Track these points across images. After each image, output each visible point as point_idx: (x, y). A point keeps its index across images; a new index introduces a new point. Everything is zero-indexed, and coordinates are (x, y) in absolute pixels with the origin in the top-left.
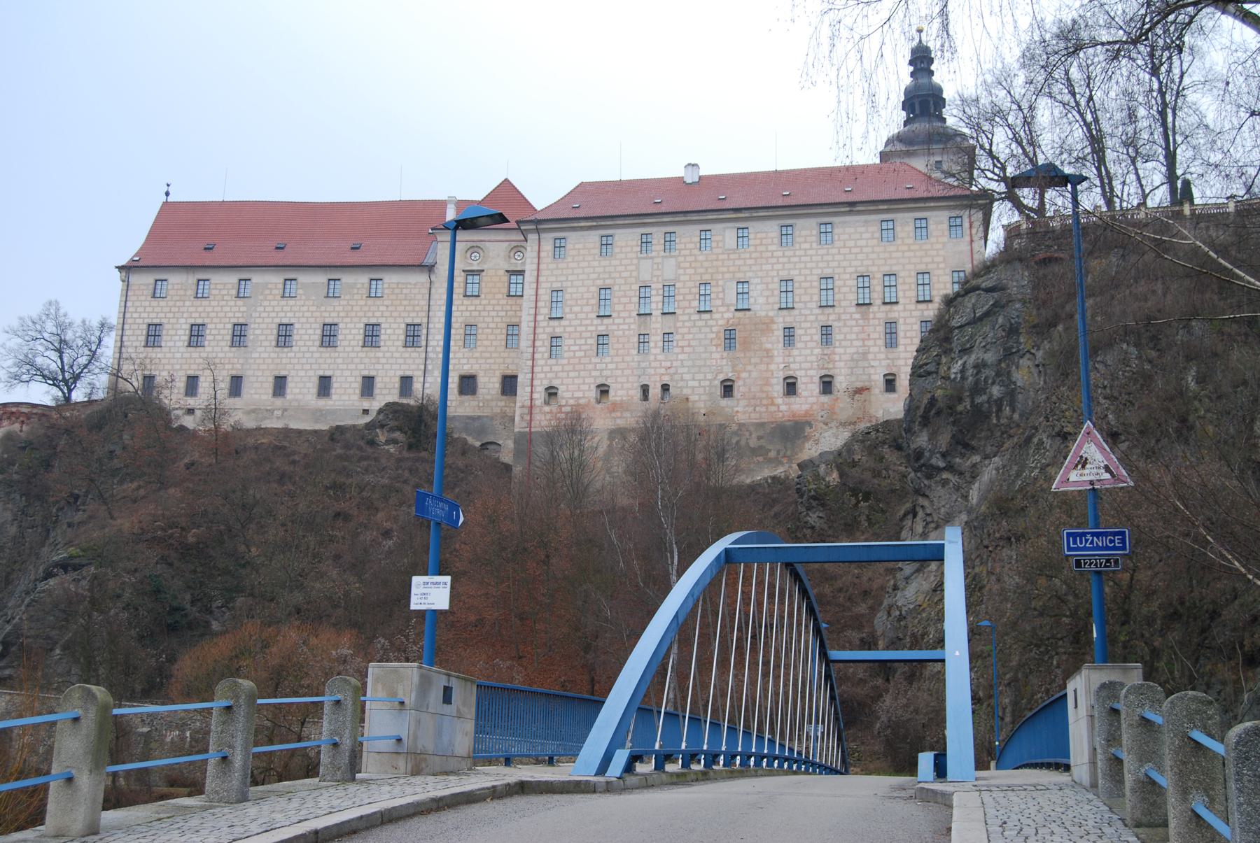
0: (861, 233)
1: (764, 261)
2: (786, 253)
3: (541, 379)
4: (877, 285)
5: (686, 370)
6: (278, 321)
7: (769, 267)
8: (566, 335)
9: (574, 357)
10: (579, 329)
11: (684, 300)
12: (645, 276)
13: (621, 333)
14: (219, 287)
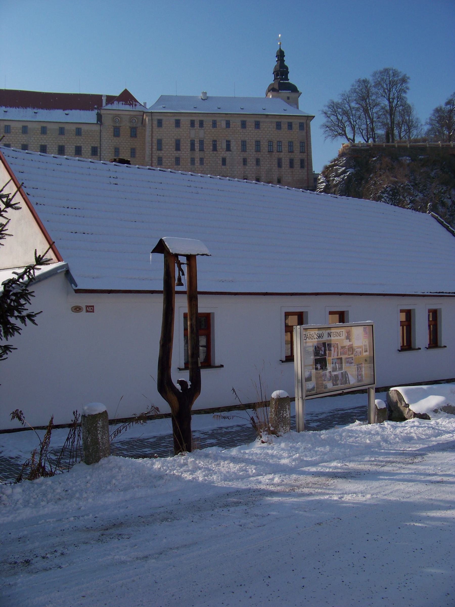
2: (244, 131)
6: (40, 144)
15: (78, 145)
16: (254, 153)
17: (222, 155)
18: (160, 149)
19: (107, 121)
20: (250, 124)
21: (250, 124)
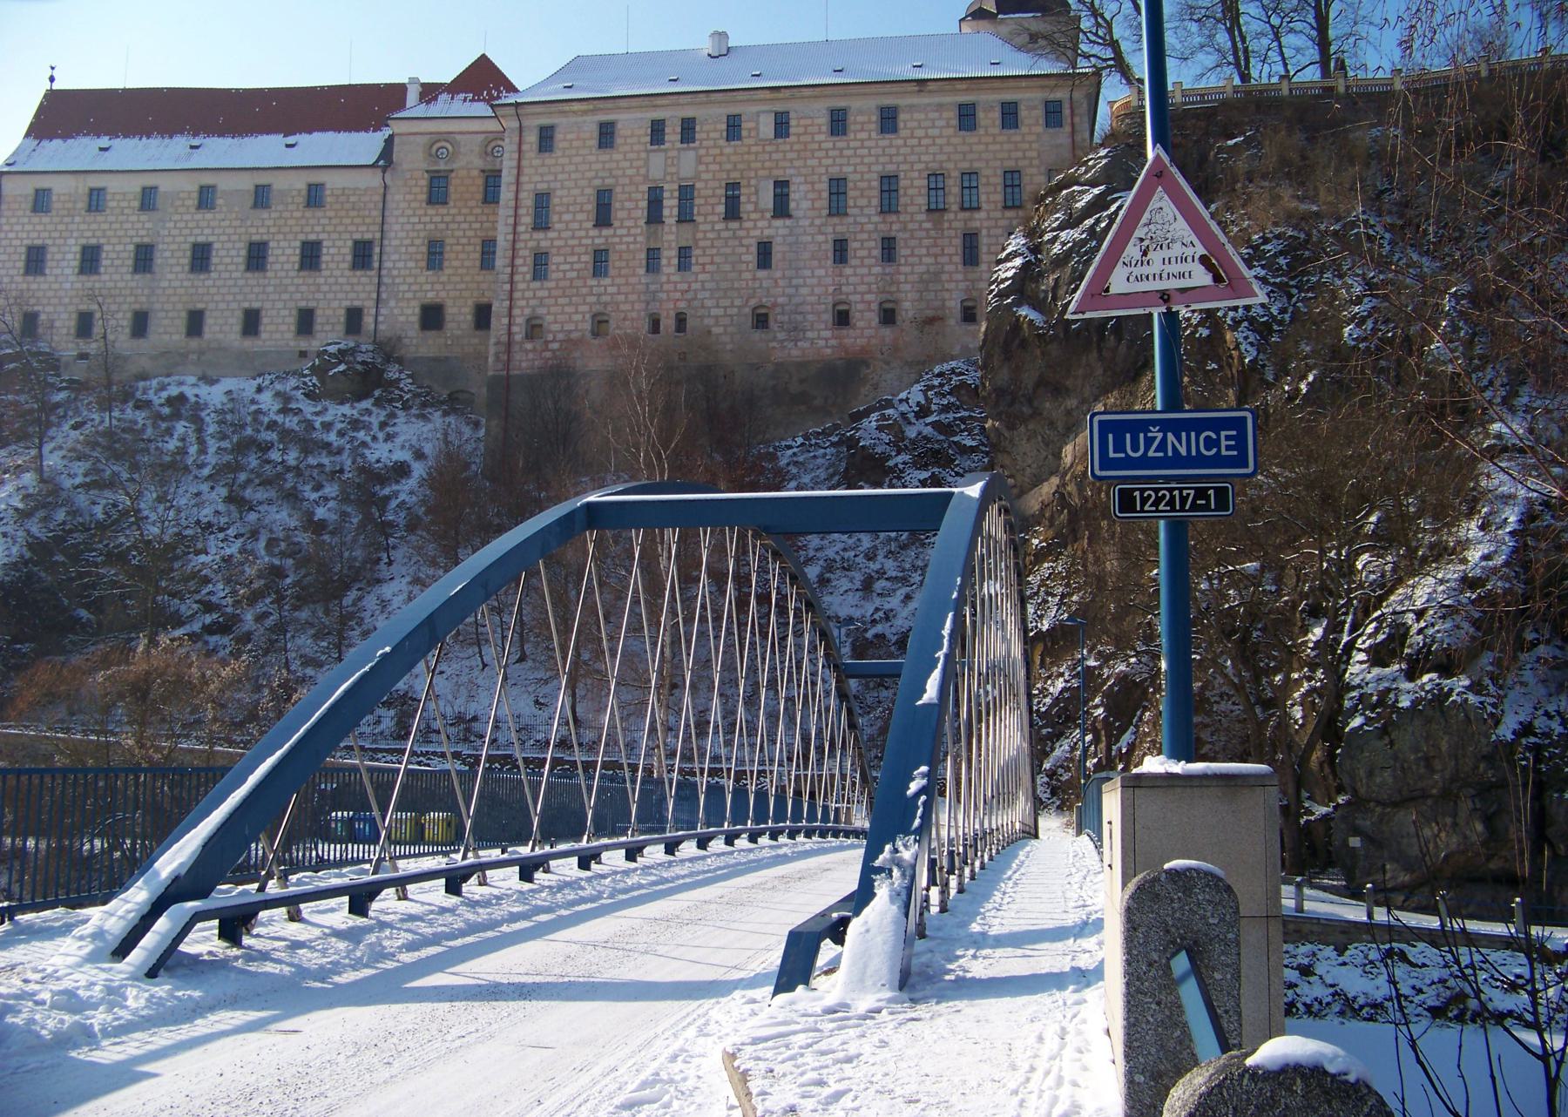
0: (933, 120)
1: (809, 154)
3: (522, 308)
4: (954, 189)
5: (707, 294)
6: (192, 239)
7: (815, 162)
8: (554, 251)
9: (564, 278)
10: (571, 242)
11: (706, 204)
12: (656, 172)
15: (312, 237)
16: (876, 219)
17: (757, 233)
18: (541, 223)
19: (412, 159)
20: (860, 119)
21: (860, 119)
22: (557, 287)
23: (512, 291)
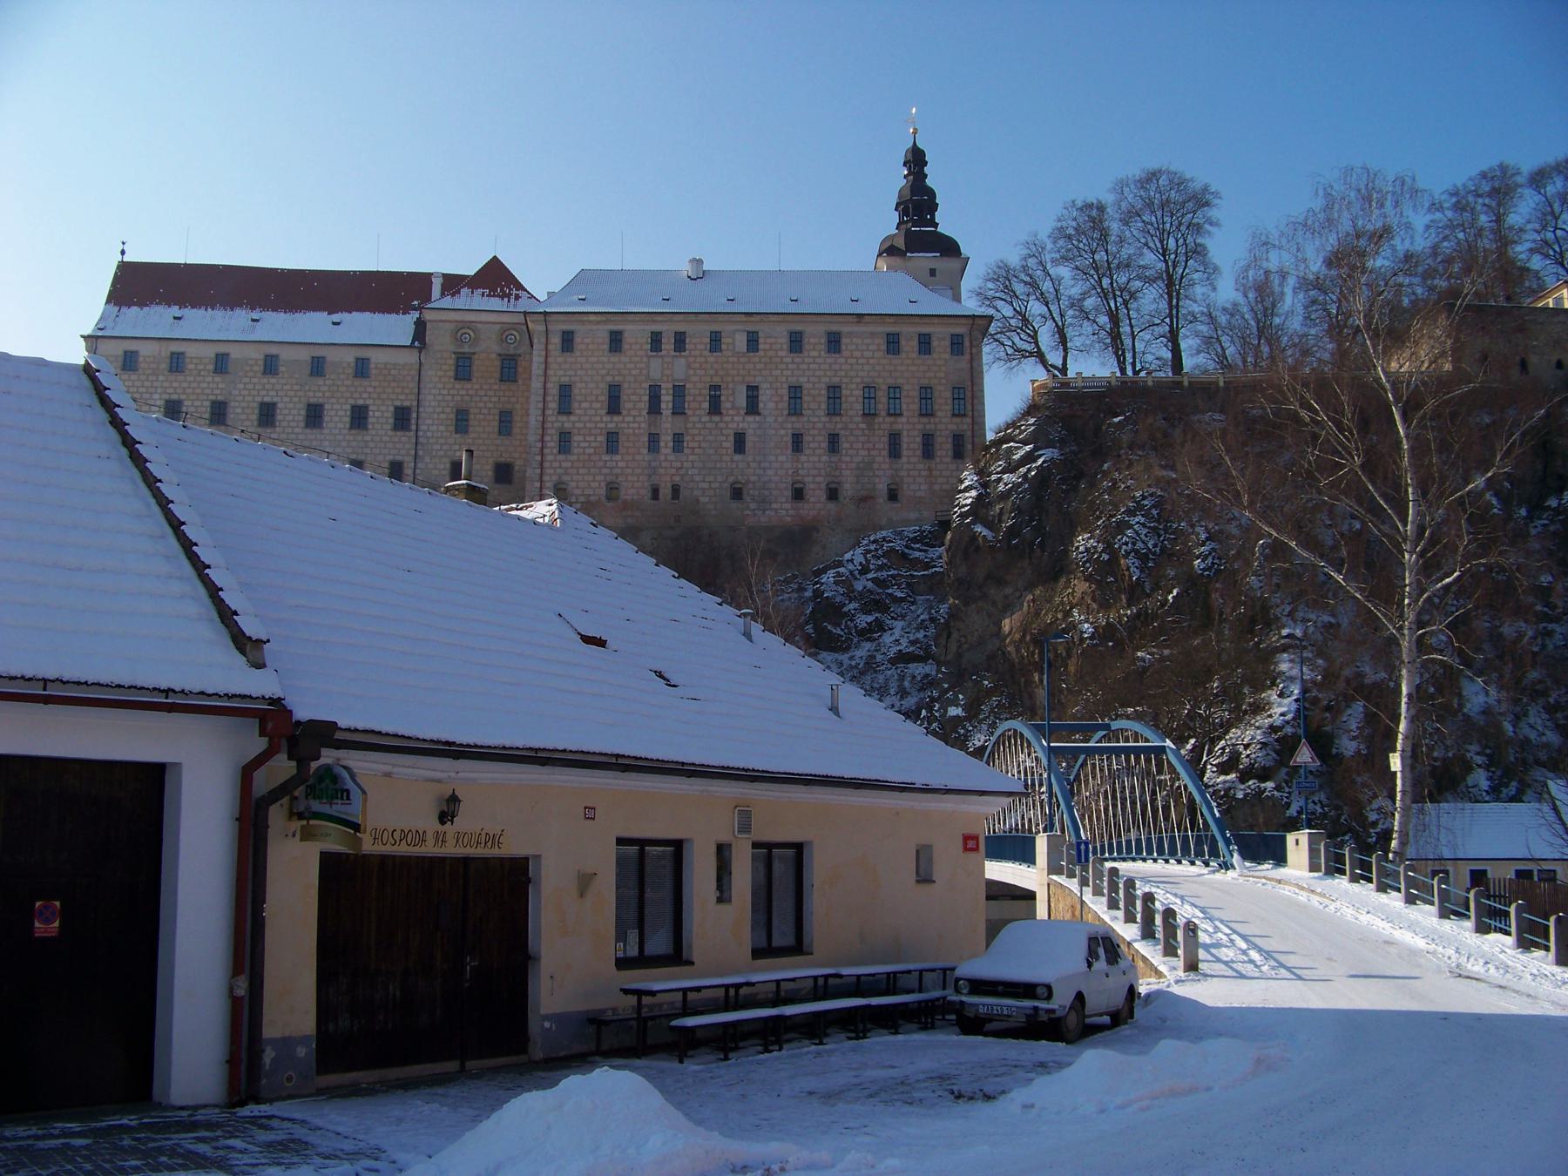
0: (868, 345)
1: (773, 366)
3: (551, 475)
5: (696, 471)
8: (576, 431)
11: (694, 401)
13: (631, 431)
14: (195, 361)
15: (361, 402)
16: (824, 419)
17: (735, 425)
18: (565, 408)
19: (440, 340)
20: (812, 340)
22: (578, 460)
23: (542, 462)
